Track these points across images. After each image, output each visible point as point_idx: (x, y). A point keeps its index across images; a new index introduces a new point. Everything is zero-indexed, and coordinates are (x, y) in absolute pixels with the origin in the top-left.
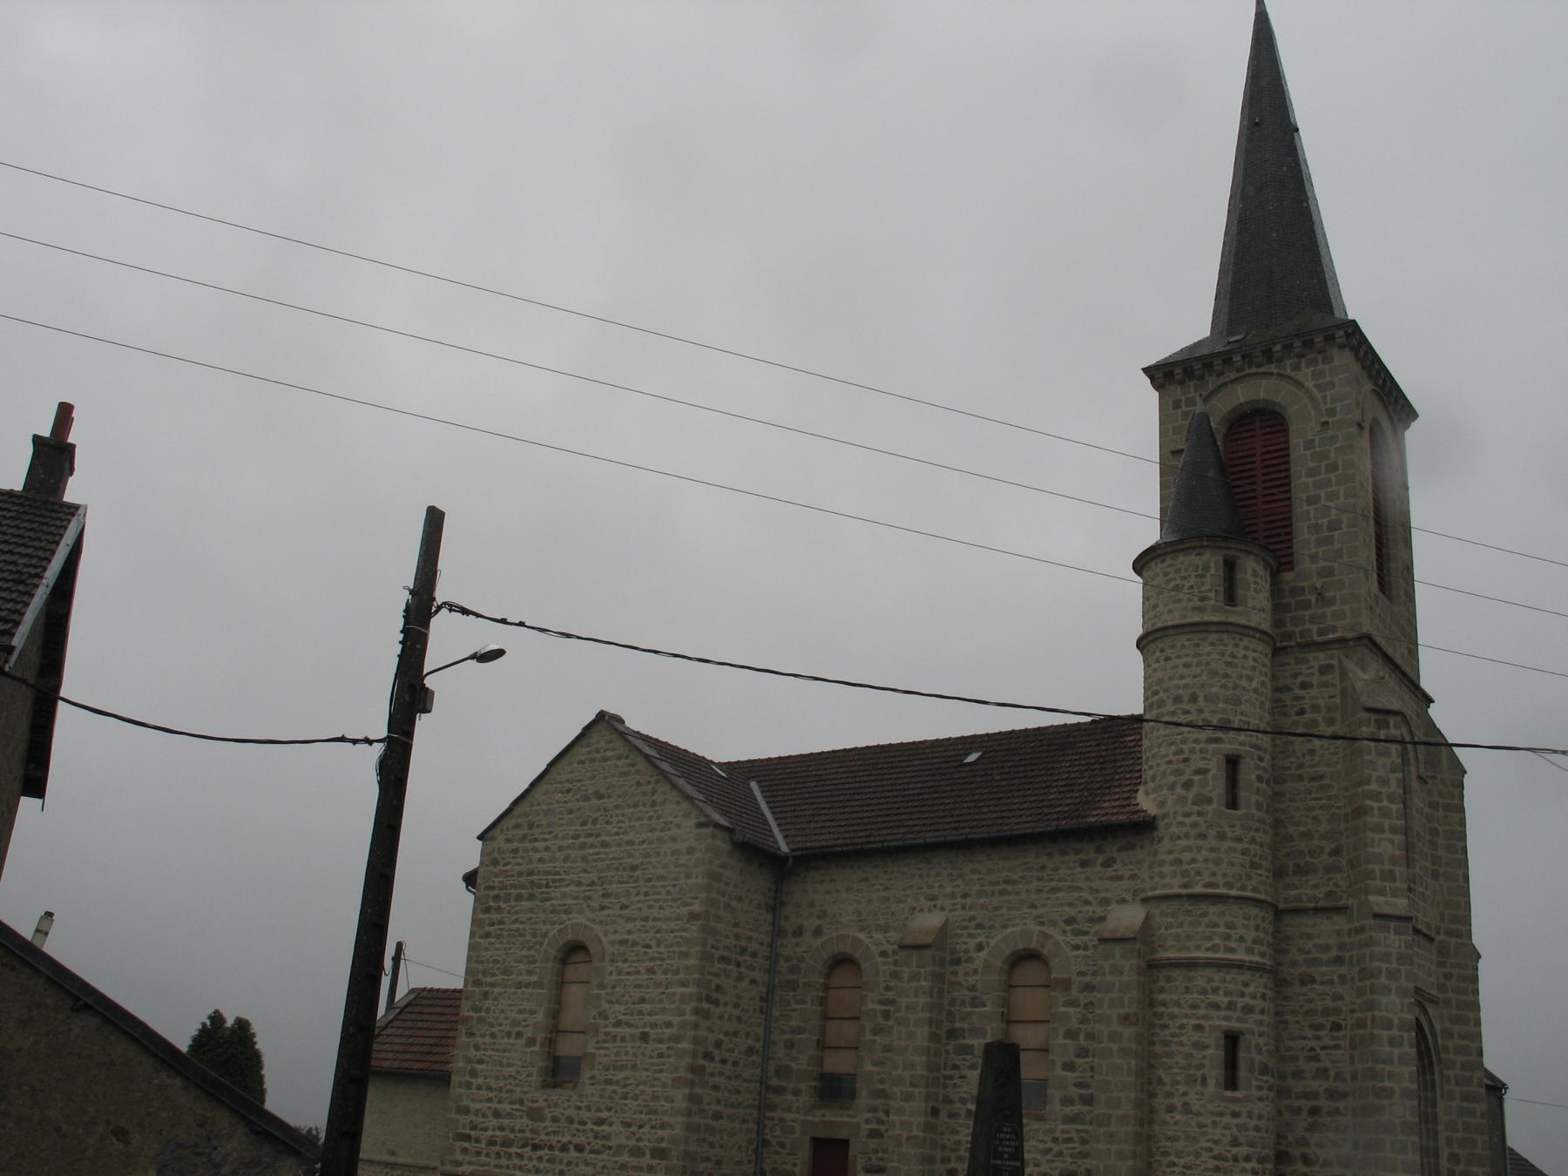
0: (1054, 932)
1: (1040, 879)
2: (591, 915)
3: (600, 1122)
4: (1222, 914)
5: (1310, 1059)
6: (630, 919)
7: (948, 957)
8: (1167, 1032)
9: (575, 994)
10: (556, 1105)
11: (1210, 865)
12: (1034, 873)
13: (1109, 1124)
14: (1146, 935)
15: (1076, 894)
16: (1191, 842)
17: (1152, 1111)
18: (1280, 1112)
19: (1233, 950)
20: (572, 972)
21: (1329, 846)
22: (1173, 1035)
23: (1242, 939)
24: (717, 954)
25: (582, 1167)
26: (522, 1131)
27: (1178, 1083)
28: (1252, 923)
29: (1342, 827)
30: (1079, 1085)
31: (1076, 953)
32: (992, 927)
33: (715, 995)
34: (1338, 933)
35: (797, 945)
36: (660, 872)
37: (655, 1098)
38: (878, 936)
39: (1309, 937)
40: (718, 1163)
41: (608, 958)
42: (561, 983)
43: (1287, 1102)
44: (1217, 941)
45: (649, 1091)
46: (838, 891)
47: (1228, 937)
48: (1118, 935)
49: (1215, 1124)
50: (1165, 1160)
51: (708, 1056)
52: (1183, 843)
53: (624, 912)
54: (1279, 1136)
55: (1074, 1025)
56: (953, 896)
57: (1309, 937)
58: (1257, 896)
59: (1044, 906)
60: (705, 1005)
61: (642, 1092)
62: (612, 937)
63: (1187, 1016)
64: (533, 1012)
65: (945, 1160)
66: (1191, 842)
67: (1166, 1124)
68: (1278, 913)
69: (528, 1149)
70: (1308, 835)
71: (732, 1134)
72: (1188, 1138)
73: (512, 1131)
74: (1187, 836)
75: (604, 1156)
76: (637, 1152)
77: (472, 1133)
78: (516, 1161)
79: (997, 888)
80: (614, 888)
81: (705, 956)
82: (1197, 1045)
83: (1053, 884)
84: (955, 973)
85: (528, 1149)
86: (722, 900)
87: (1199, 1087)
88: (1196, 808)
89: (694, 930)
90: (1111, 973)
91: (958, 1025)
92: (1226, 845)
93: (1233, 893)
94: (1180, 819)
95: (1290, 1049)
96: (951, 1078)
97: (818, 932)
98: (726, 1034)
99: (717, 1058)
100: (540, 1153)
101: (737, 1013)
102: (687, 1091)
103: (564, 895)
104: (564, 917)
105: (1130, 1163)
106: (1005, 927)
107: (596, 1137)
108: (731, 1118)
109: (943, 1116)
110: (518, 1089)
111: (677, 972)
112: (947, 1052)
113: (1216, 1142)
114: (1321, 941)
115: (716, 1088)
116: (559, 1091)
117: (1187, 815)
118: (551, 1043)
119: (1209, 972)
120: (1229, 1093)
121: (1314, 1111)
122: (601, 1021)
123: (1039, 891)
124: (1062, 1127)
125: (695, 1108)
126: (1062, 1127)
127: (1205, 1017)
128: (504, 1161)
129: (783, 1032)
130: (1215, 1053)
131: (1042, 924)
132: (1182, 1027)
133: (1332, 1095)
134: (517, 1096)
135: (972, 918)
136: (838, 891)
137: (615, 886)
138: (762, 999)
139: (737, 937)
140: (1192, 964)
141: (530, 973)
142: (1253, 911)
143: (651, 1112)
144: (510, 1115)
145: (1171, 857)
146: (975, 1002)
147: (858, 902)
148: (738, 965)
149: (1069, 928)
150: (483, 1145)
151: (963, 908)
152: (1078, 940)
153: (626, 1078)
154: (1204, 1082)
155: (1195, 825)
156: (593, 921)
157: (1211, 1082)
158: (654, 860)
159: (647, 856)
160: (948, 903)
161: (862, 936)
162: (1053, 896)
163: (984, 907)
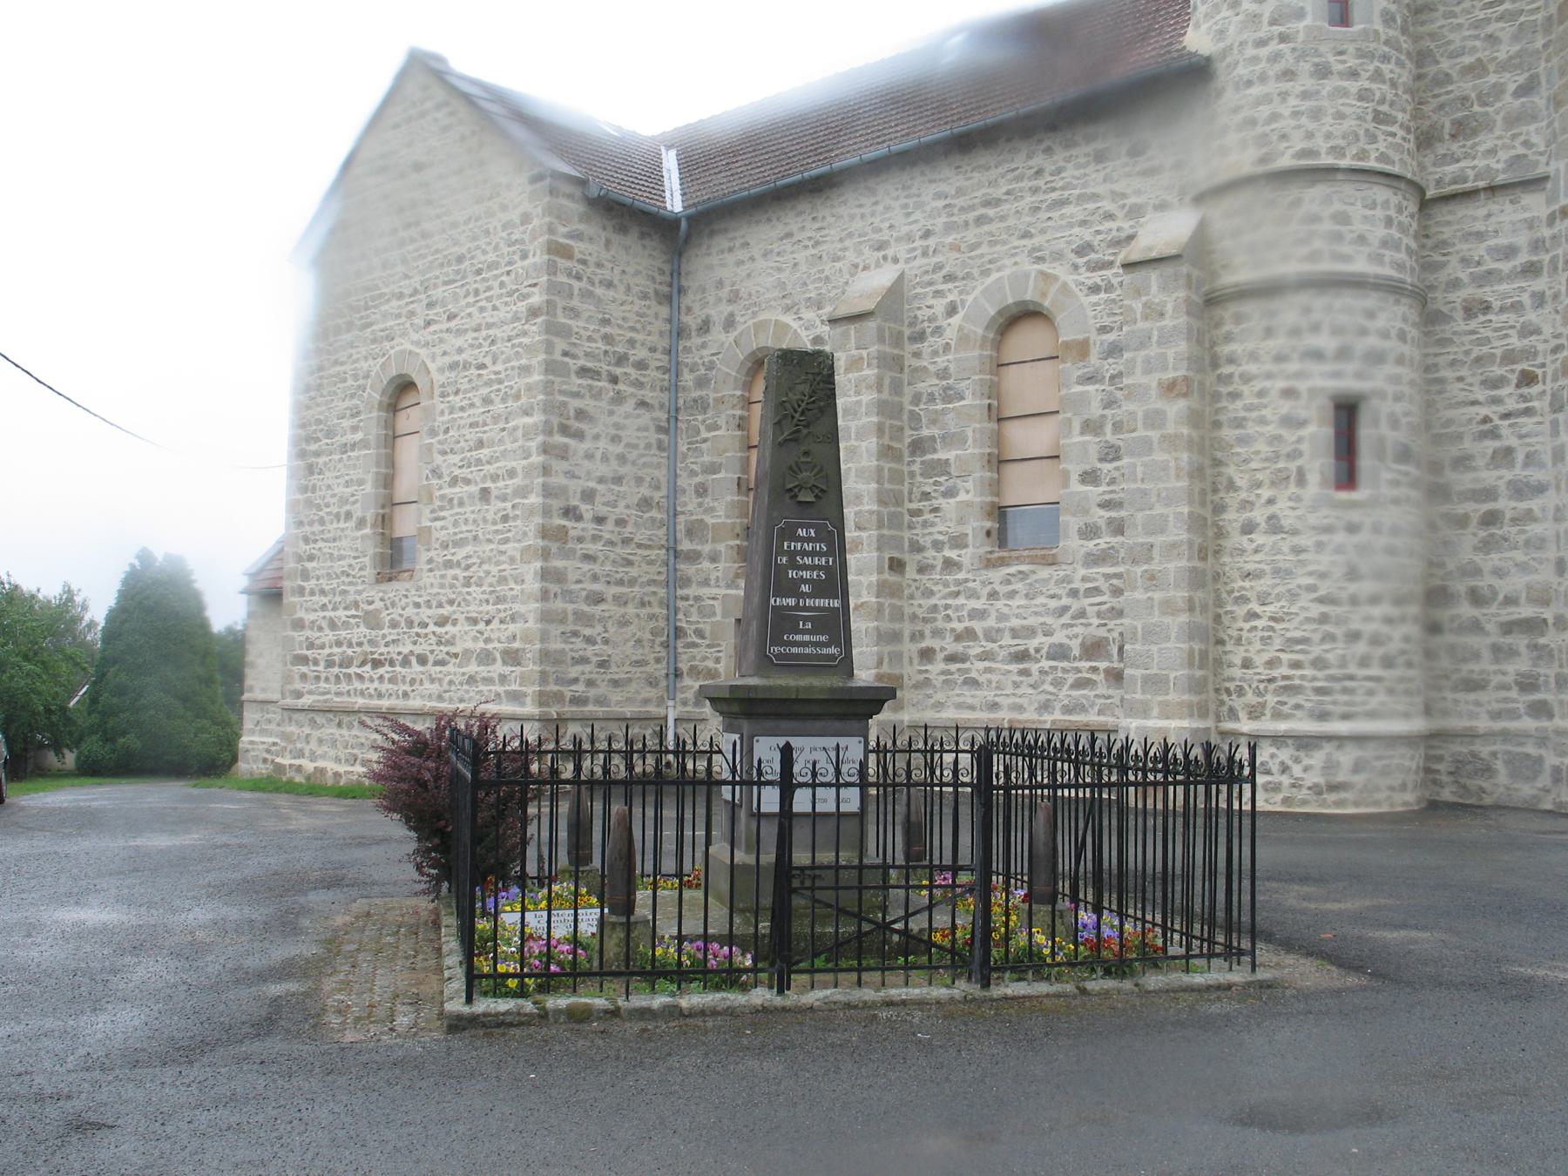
0: (1060, 271)
1: (1035, 191)
2: (415, 337)
3: (442, 622)
4: (1327, 200)
5: (1483, 435)
6: (460, 332)
7: (907, 332)
8: (1239, 404)
9: (408, 452)
10: (393, 604)
11: (1304, 120)
12: (1026, 184)
13: (1149, 560)
14: (1198, 251)
15: (1091, 206)
16: (1272, 87)
17: (1220, 533)
18: (1432, 526)
19: (1346, 258)
20: (406, 421)
21: (1513, 81)
22: (1249, 408)
23: (1362, 239)
24: (574, 364)
25: (427, 685)
26: (360, 644)
27: (1259, 485)
28: (1379, 213)
29: (1539, 44)
30: (1106, 505)
31: (1094, 298)
32: (968, 276)
33: (575, 425)
34: (1531, 224)
35: (704, 346)
36: (491, 257)
37: (503, 580)
38: (808, 315)
39: (1480, 236)
40: (603, 664)
41: (437, 392)
42: (391, 439)
43: (1446, 508)
44: (1318, 244)
45: (494, 570)
46: (752, 259)
47: (1338, 237)
48: (1154, 255)
49: (1320, 546)
50: (1241, 611)
51: (569, 512)
52: (1256, 91)
53: (452, 324)
54: (1431, 564)
55: (1096, 410)
56: (909, 238)
57: (1480, 236)
58: (1388, 168)
59: (1043, 231)
60: (559, 439)
61: (488, 573)
62: (441, 361)
63: (1269, 376)
64: (361, 482)
65: (917, 636)
66: (1272, 87)
67: (1242, 551)
68: (1426, 205)
69: (368, 667)
70: (1478, 69)
71: (624, 623)
72: (1277, 572)
73: (350, 645)
74: (1263, 78)
75: (450, 668)
76: (486, 658)
77: (309, 653)
78: (357, 685)
79: (971, 216)
80: (437, 293)
81: (550, 367)
82: (1290, 422)
83: (1055, 195)
84: (917, 355)
85: (368, 667)
86: (576, 284)
87: (1293, 489)
88: (1277, 29)
89: (535, 327)
90: (1146, 318)
91: (925, 432)
92: (1329, 85)
93: (1345, 163)
94: (1250, 51)
95: (1449, 422)
96: (918, 513)
97: (730, 323)
98: (601, 480)
99: (588, 516)
100: (381, 671)
101: (618, 449)
102: (538, 564)
103: (385, 316)
104: (387, 345)
105: (1184, 618)
106: (986, 273)
107: (439, 643)
108: (621, 601)
109: (911, 572)
110: (351, 589)
111: (517, 397)
112: (912, 475)
113: (1323, 576)
114: (1502, 241)
115: (588, 558)
116: (395, 585)
117: (1261, 43)
118: (385, 520)
119: (1302, 298)
120: (1343, 495)
121: (1491, 519)
122: (435, 482)
123: (1035, 209)
124: (1082, 572)
125: (554, 588)
126: (1082, 572)
127: (1299, 375)
128: (344, 687)
129: (693, 473)
130: (1318, 432)
131: (1041, 259)
132: (1261, 393)
133: (1520, 490)
134: (350, 598)
135: (938, 267)
136: (752, 259)
137: (440, 290)
138: (660, 429)
139: (608, 339)
140: (1269, 290)
141: (355, 429)
142: (1381, 193)
143: (499, 600)
144: (346, 625)
145: (1239, 117)
146: (950, 395)
147: (779, 270)
148: (614, 380)
149: (1081, 261)
150: (321, 668)
151: (925, 254)
152: (1096, 278)
153: (468, 557)
154: (1301, 480)
155: (1275, 57)
156: (417, 343)
157: (1313, 479)
158: (482, 242)
159: (475, 238)
160: (900, 250)
161: (788, 319)
162: (1055, 214)
163: (955, 248)
